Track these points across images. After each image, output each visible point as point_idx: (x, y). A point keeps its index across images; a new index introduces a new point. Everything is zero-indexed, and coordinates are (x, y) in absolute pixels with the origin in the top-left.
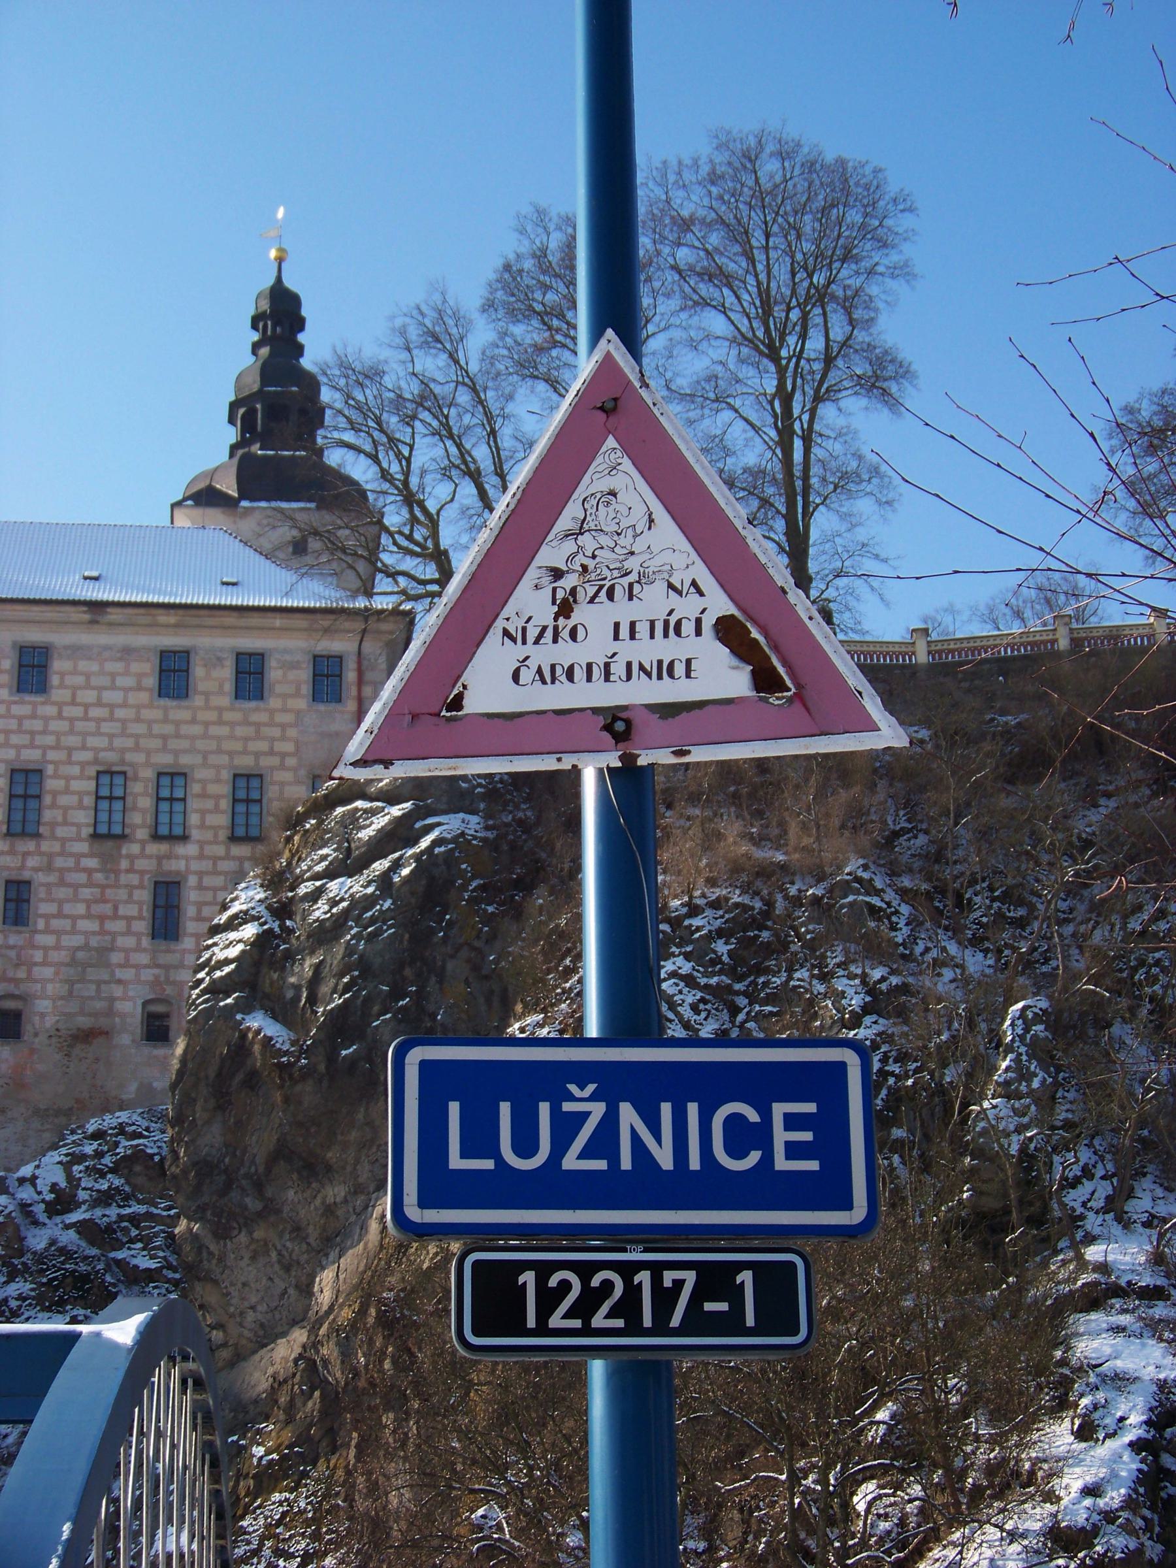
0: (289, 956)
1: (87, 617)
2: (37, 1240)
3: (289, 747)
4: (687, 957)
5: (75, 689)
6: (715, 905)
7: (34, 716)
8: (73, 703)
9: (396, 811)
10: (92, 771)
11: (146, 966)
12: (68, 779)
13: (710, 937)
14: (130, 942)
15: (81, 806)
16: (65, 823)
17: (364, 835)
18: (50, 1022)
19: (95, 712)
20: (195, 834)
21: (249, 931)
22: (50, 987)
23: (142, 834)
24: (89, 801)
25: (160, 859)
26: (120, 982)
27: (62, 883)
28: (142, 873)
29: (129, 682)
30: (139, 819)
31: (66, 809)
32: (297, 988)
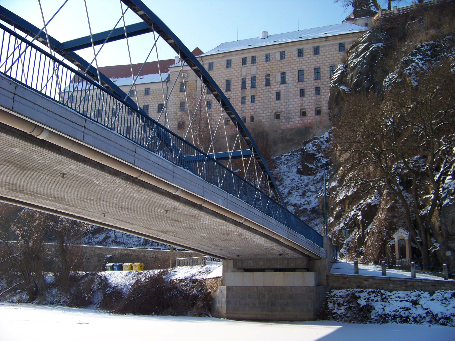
0: (347, 74)
1: (325, 40)
2: (323, 147)
4: (421, 55)
5: (324, 53)
6: (427, 45)
7: (317, 59)
8: (324, 55)
9: (365, 44)
10: (329, 66)
12: (325, 68)
13: (426, 51)
15: (327, 73)
16: (325, 76)
17: (360, 50)
19: (328, 56)
21: (340, 72)
22: (325, 105)
24: (329, 72)
27: (325, 86)
29: (334, 50)
31: (325, 74)
32: (349, 80)
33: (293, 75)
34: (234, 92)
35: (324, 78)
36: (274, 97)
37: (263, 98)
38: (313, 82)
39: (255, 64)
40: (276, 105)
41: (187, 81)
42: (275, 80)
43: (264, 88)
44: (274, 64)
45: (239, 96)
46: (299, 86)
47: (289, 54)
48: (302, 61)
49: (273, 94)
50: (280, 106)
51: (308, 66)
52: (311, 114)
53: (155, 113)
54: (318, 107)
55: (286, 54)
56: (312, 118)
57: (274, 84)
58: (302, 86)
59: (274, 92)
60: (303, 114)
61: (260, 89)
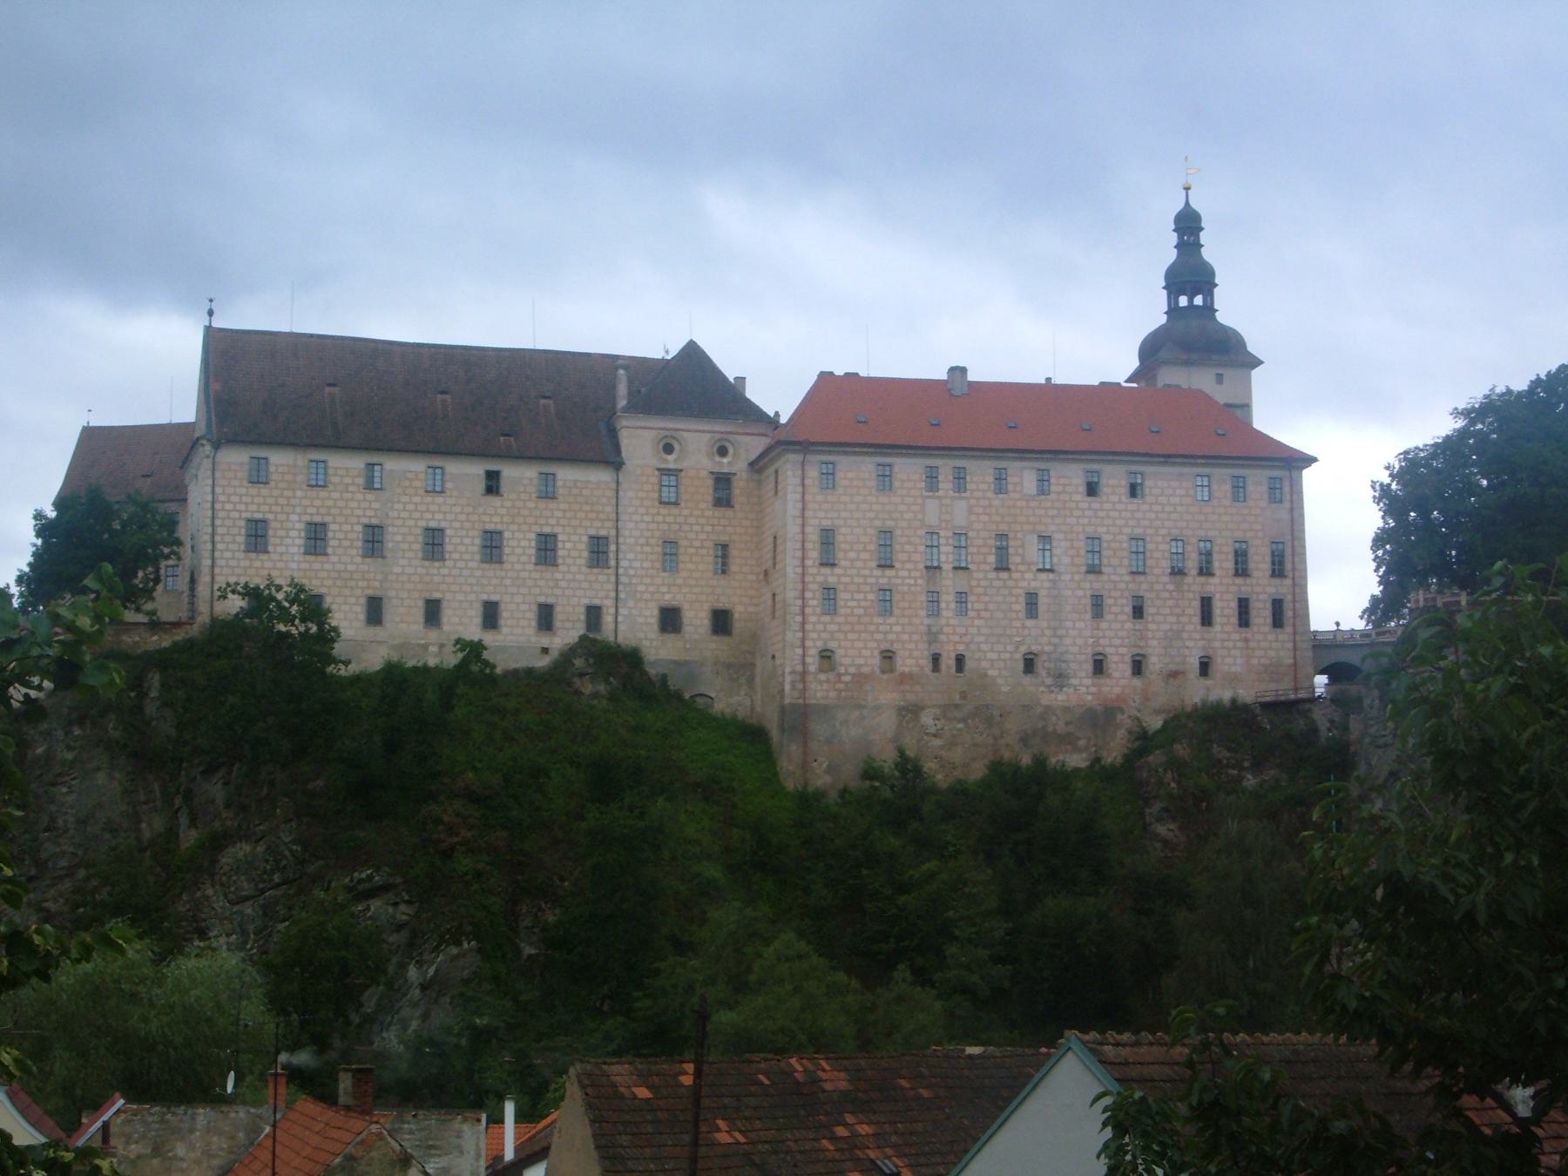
3: (1260, 527)
10: (1168, 539)
11: (1199, 640)
14: (1190, 628)
18: (1158, 667)
20: (1217, 572)
23: (1194, 572)
24: (1167, 555)
25: (1202, 584)
26: (1188, 647)
27: (1158, 598)
28: (1194, 592)
29: (1183, 492)
30: (1192, 565)
33: (1072, 547)
34: (905, 573)
35: (1156, 571)
36: (1020, 606)
37: (991, 607)
38: (1127, 578)
39: (963, 495)
40: (1026, 632)
41: (681, 470)
42: (1023, 556)
43: (992, 575)
44: (1019, 503)
45: (918, 588)
46: (1088, 585)
47: (1062, 481)
48: (1096, 510)
49: (1017, 596)
50: (1036, 636)
51: (1112, 529)
52: (1120, 669)
53: (580, 566)
54: (1138, 655)
55: (1053, 481)
56: (1123, 682)
57: (1022, 568)
58: (1097, 586)
59: (1021, 592)
60: (1099, 667)
61: (981, 575)
